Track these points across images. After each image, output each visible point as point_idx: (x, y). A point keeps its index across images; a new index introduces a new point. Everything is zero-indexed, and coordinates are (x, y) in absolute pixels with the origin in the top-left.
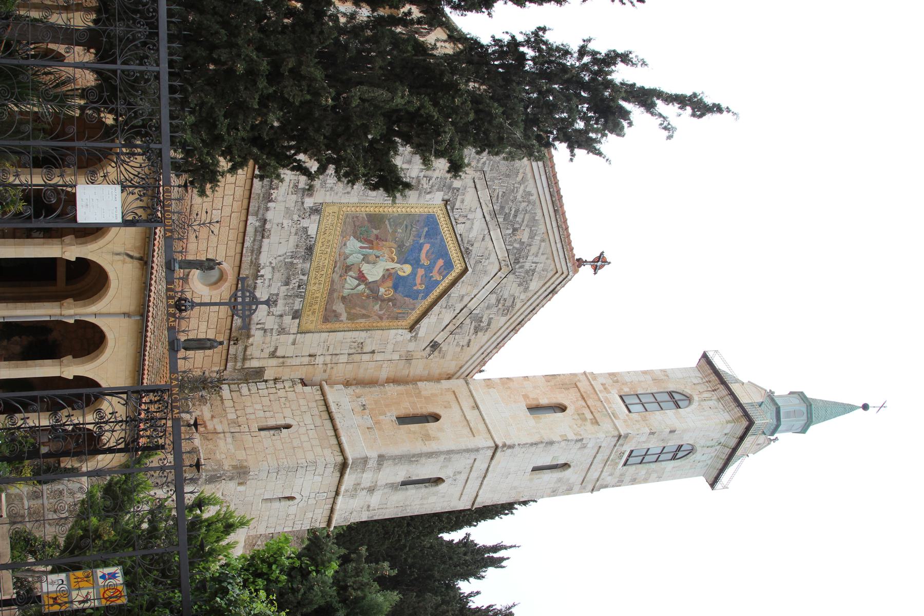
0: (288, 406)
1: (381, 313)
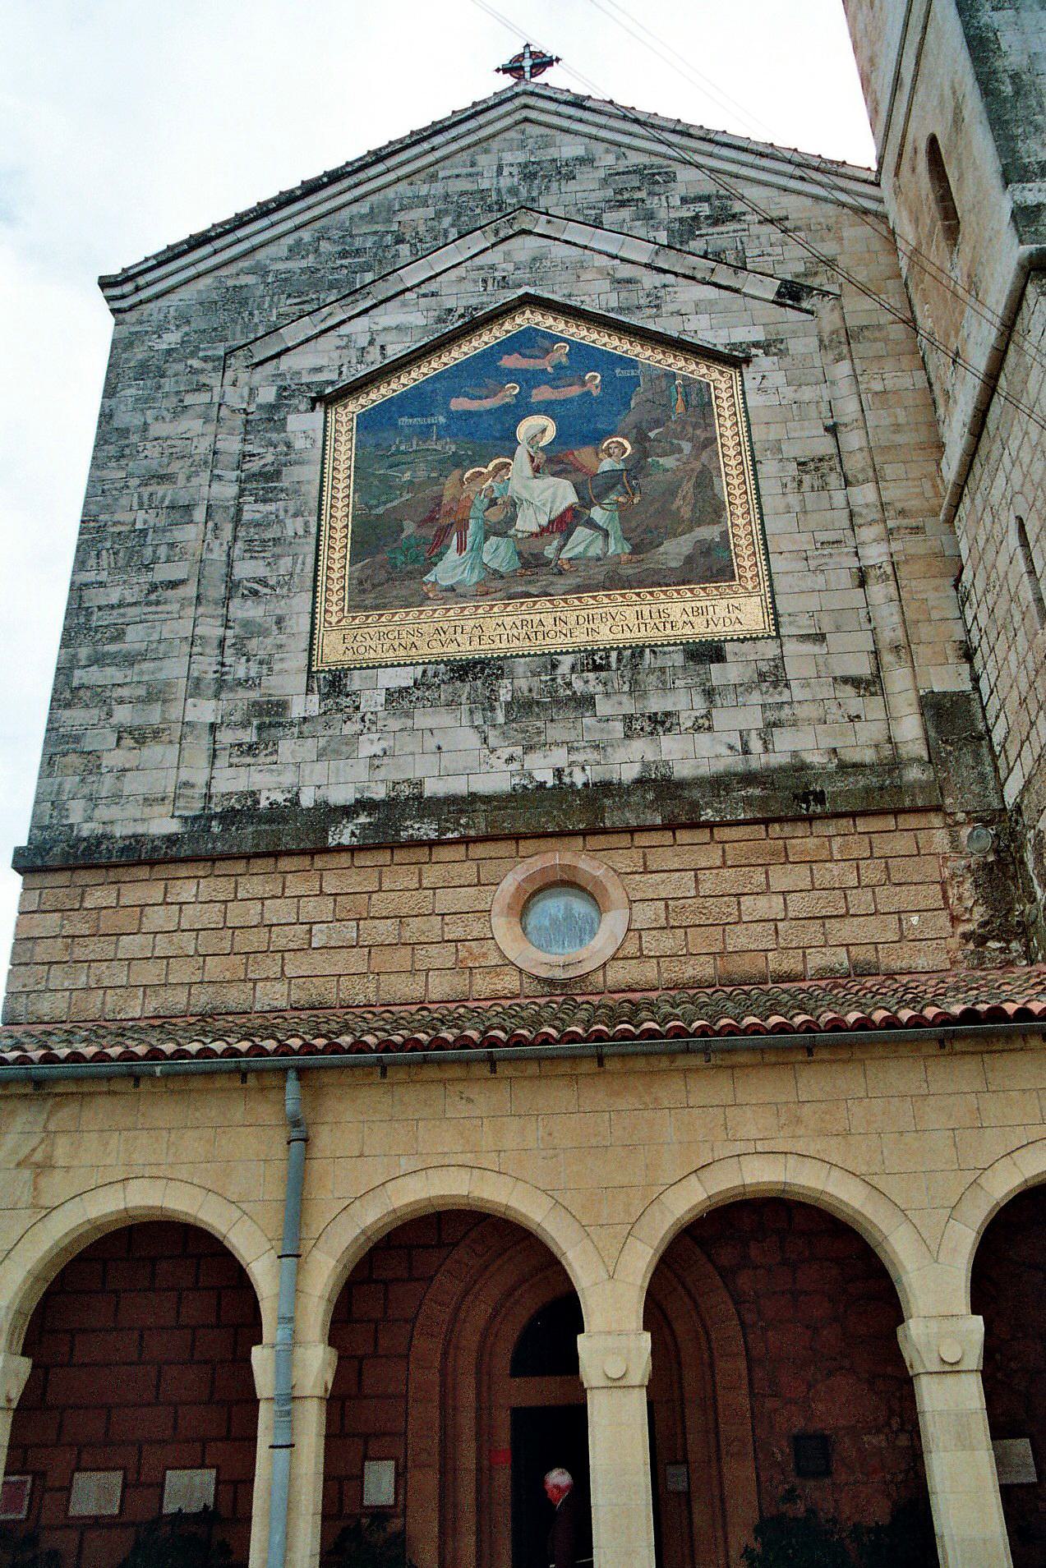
1: (687, 447)
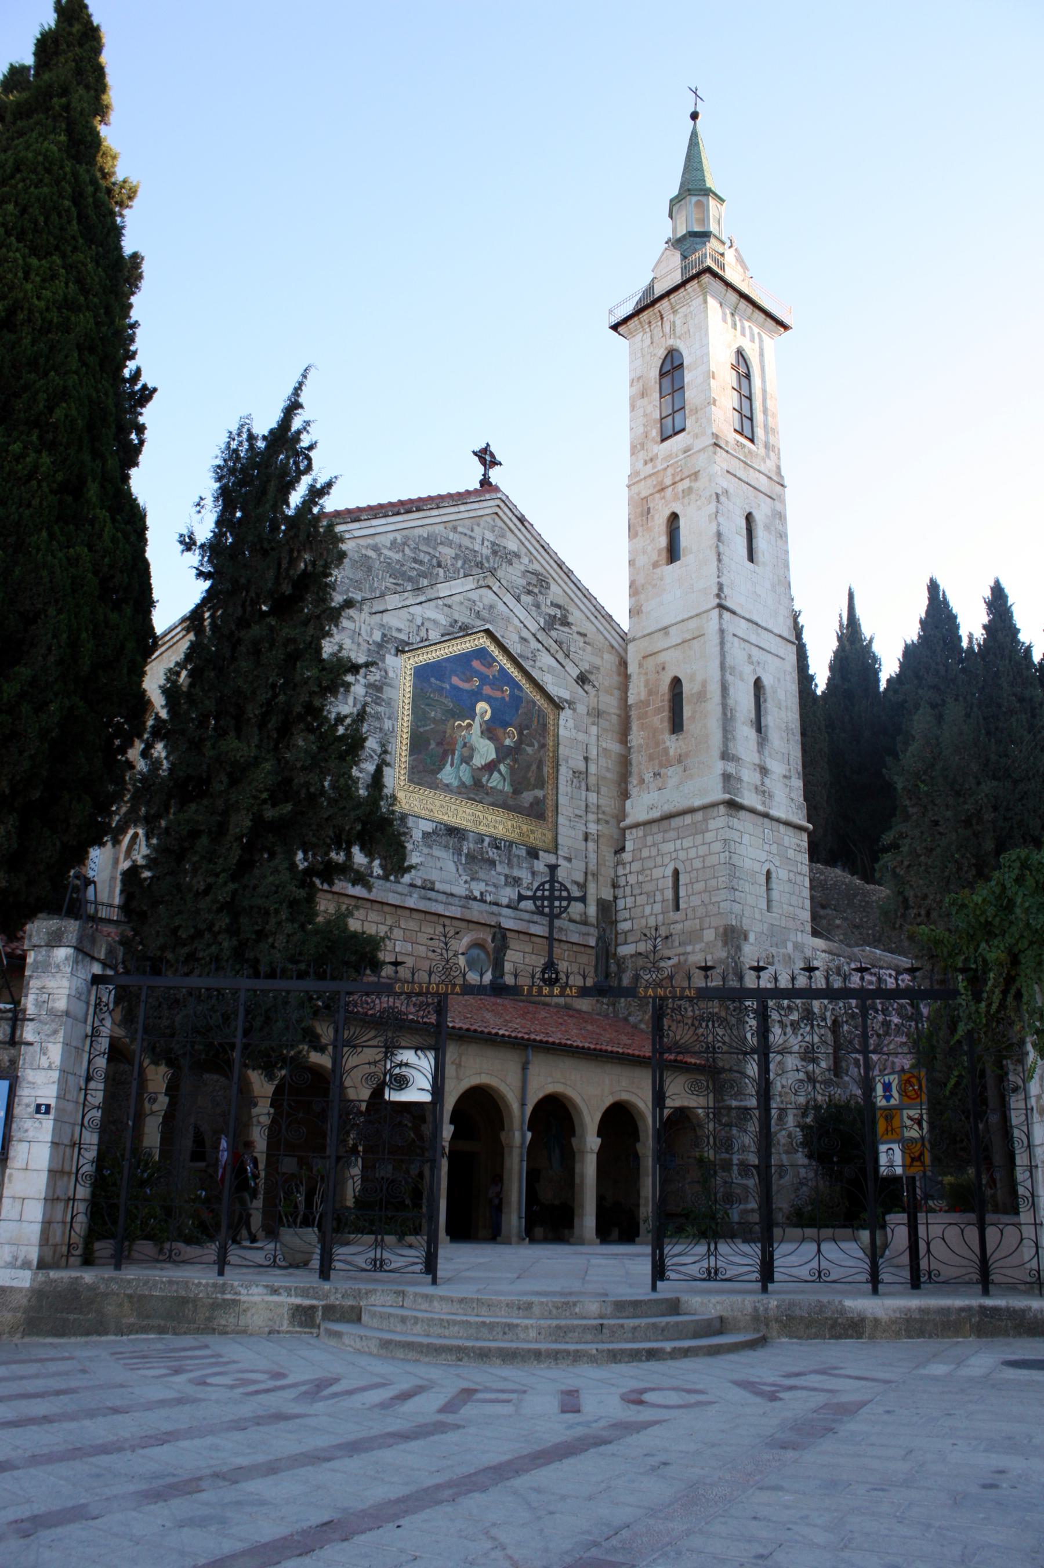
0: (648, 872)
1: (536, 745)
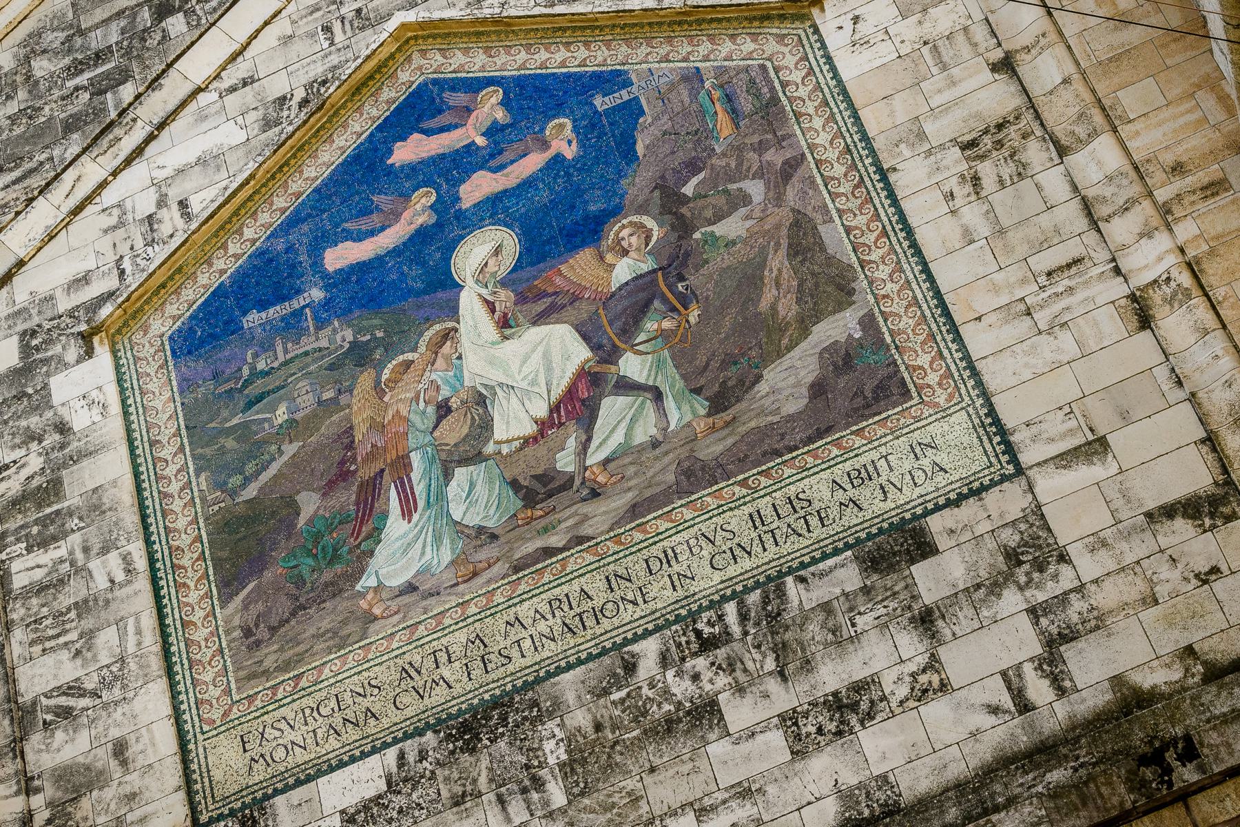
1: (755, 189)
